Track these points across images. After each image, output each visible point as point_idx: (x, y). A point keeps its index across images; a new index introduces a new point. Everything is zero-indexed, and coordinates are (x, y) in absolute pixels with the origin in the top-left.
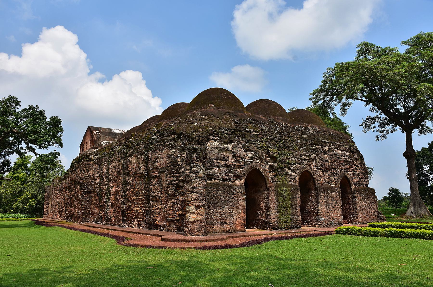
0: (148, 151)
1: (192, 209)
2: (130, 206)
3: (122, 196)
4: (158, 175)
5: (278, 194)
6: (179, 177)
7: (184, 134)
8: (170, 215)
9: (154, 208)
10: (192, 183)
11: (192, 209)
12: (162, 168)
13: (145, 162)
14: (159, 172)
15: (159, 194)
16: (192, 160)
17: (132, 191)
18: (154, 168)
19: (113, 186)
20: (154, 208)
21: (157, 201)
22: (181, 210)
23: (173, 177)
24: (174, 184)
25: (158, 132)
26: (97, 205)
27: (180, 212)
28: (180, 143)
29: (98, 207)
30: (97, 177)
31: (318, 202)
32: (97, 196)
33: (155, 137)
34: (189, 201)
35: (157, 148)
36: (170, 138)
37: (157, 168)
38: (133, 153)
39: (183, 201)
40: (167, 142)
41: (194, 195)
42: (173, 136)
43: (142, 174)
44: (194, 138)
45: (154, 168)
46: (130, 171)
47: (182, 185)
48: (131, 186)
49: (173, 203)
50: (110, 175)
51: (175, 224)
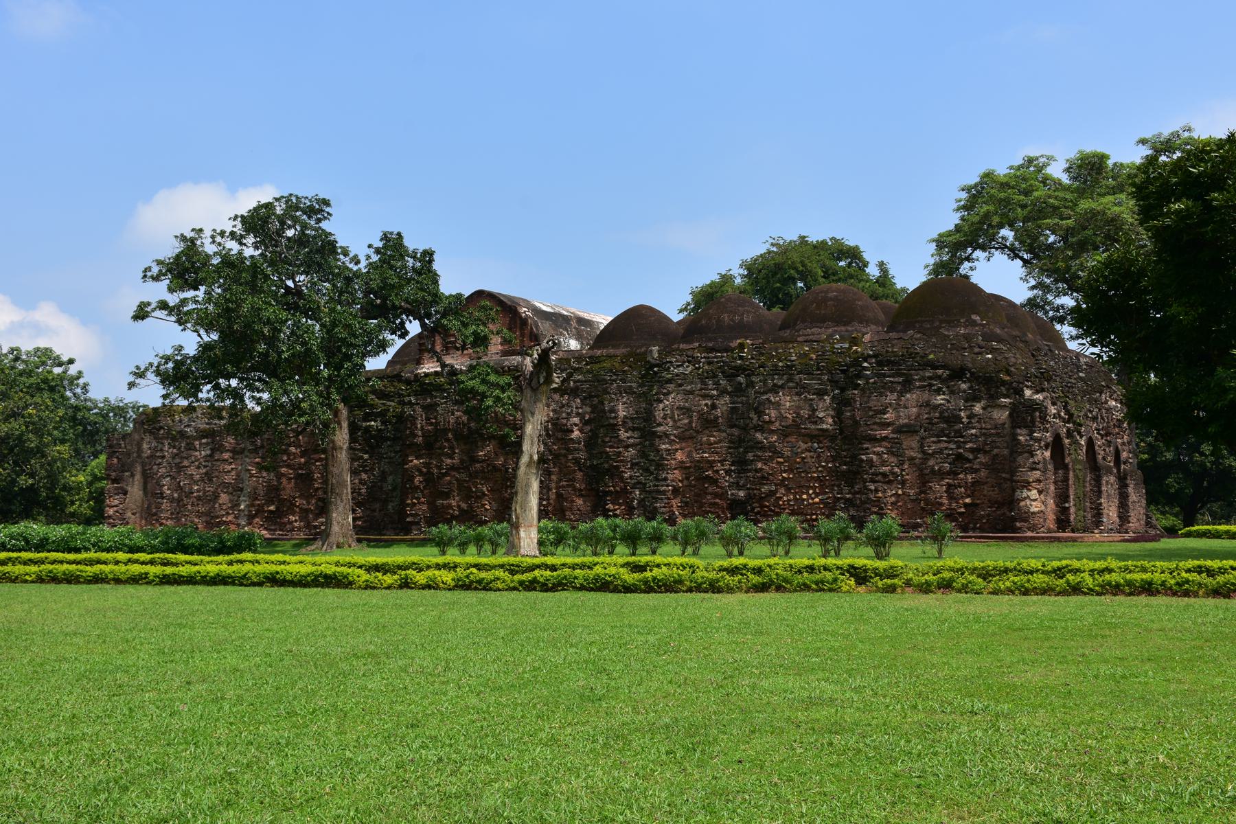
0: (843, 390)
1: (1034, 494)
2: (772, 493)
3: (728, 472)
4: (891, 436)
5: (1076, 476)
6: (965, 443)
7: (972, 374)
8: (942, 504)
9: (880, 494)
10: (1032, 456)
11: (1034, 494)
12: (903, 426)
13: (834, 409)
14: (893, 432)
15: (896, 470)
16: (1033, 421)
17: (778, 463)
18: (875, 423)
19: (677, 450)
20: (880, 494)
21: (890, 482)
22: (968, 496)
23: (948, 442)
24: (948, 455)
25: (875, 356)
26: (580, 490)
27: (968, 500)
28: (964, 386)
29: (581, 496)
30: (576, 425)
31: (1100, 492)
32: (580, 470)
33: (865, 364)
34: (1029, 483)
35: (883, 388)
36: (927, 374)
37: (889, 424)
38: (782, 387)
39: (973, 483)
40: (922, 379)
41: (1037, 474)
42: (940, 372)
43: (827, 430)
44: (1003, 383)
45: (875, 423)
46: (770, 422)
47: (971, 457)
48: (775, 452)
49: (949, 485)
50: (660, 425)
51: (955, 520)
